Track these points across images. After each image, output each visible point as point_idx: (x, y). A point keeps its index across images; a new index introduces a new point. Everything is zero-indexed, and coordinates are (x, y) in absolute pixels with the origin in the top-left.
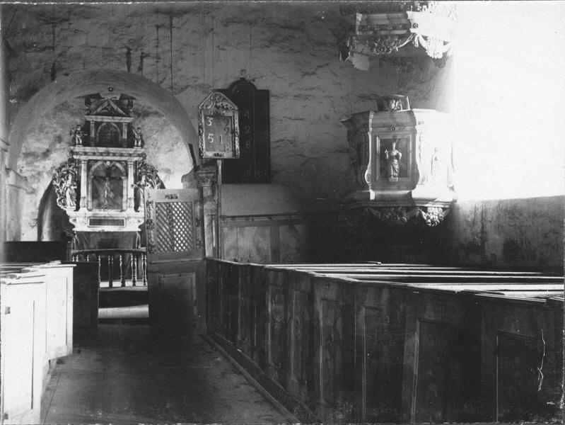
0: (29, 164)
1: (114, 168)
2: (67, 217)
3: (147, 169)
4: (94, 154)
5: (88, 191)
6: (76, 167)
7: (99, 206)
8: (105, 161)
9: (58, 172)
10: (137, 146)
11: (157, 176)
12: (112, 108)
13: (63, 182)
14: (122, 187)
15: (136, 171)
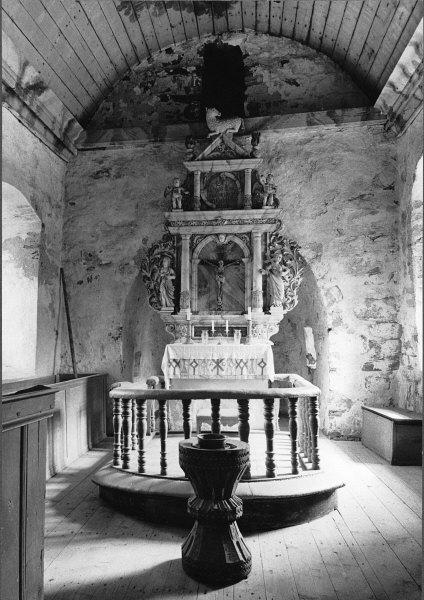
3: (282, 243)
4: (200, 223)
5: (191, 282)
6: (173, 247)
8: (217, 235)
11: (299, 255)
14: (243, 274)
15: (266, 250)
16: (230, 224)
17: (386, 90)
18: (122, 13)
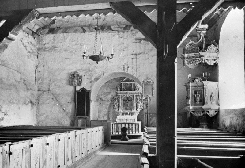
4: (123, 93)
8: (127, 95)
16: (129, 93)
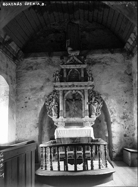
0: (33, 94)
1: (77, 94)
2: (54, 122)
4: (66, 86)
5: (63, 107)
6: (57, 95)
7: (70, 116)
8: (72, 91)
9: (48, 98)
10: (90, 80)
11: (101, 97)
12: (75, 60)
13: (50, 103)
14: (82, 104)
15: (89, 95)
17: (127, 44)
18: (37, 14)
